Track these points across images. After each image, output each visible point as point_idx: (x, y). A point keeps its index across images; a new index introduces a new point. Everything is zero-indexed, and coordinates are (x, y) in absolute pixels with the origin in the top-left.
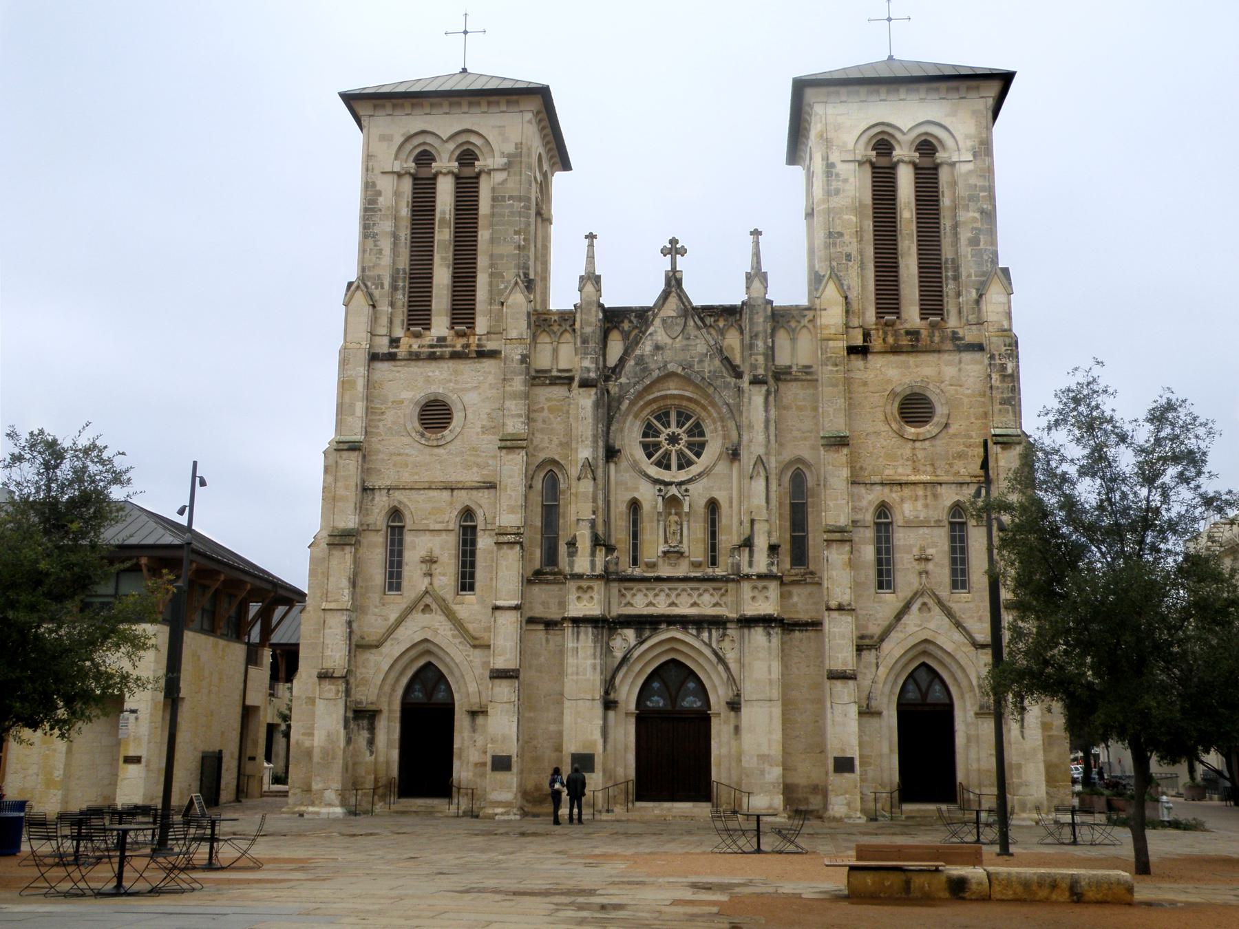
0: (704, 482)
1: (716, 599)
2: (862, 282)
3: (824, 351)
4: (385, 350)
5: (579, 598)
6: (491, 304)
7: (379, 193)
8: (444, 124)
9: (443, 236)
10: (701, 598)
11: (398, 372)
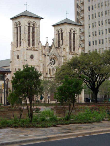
9: (31, 34)
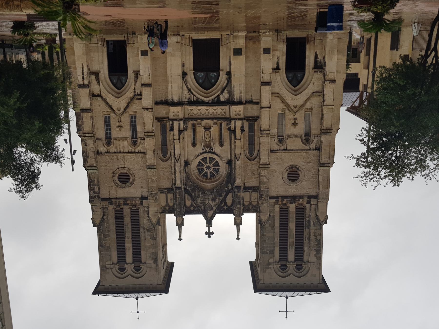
0: (197, 153)
2: (144, 221)
3: (156, 198)
4: (312, 199)
6: (274, 215)
7: (315, 255)
8: (292, 279)
9: (292, 240)
10: (197, 112)
11: (307, 192)
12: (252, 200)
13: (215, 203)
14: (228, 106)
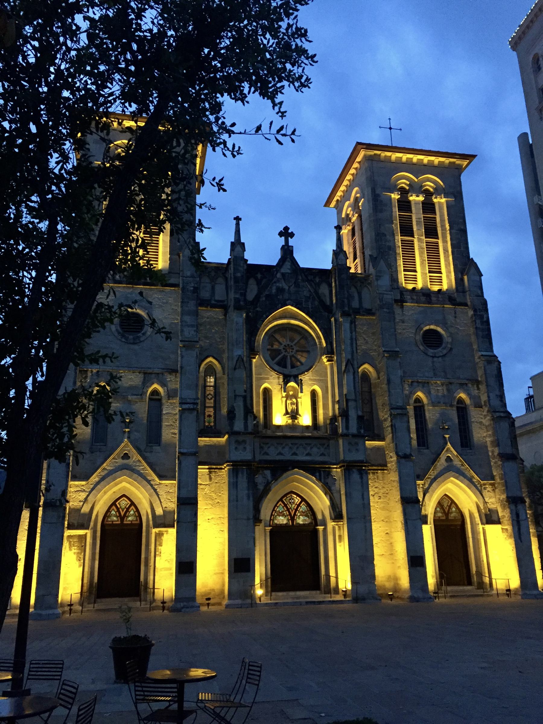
1: (322, 450)
3: (381, 300)
5: (236, 448)
12: (209, 286)
13: (278, 284)
14: (257, 459)
